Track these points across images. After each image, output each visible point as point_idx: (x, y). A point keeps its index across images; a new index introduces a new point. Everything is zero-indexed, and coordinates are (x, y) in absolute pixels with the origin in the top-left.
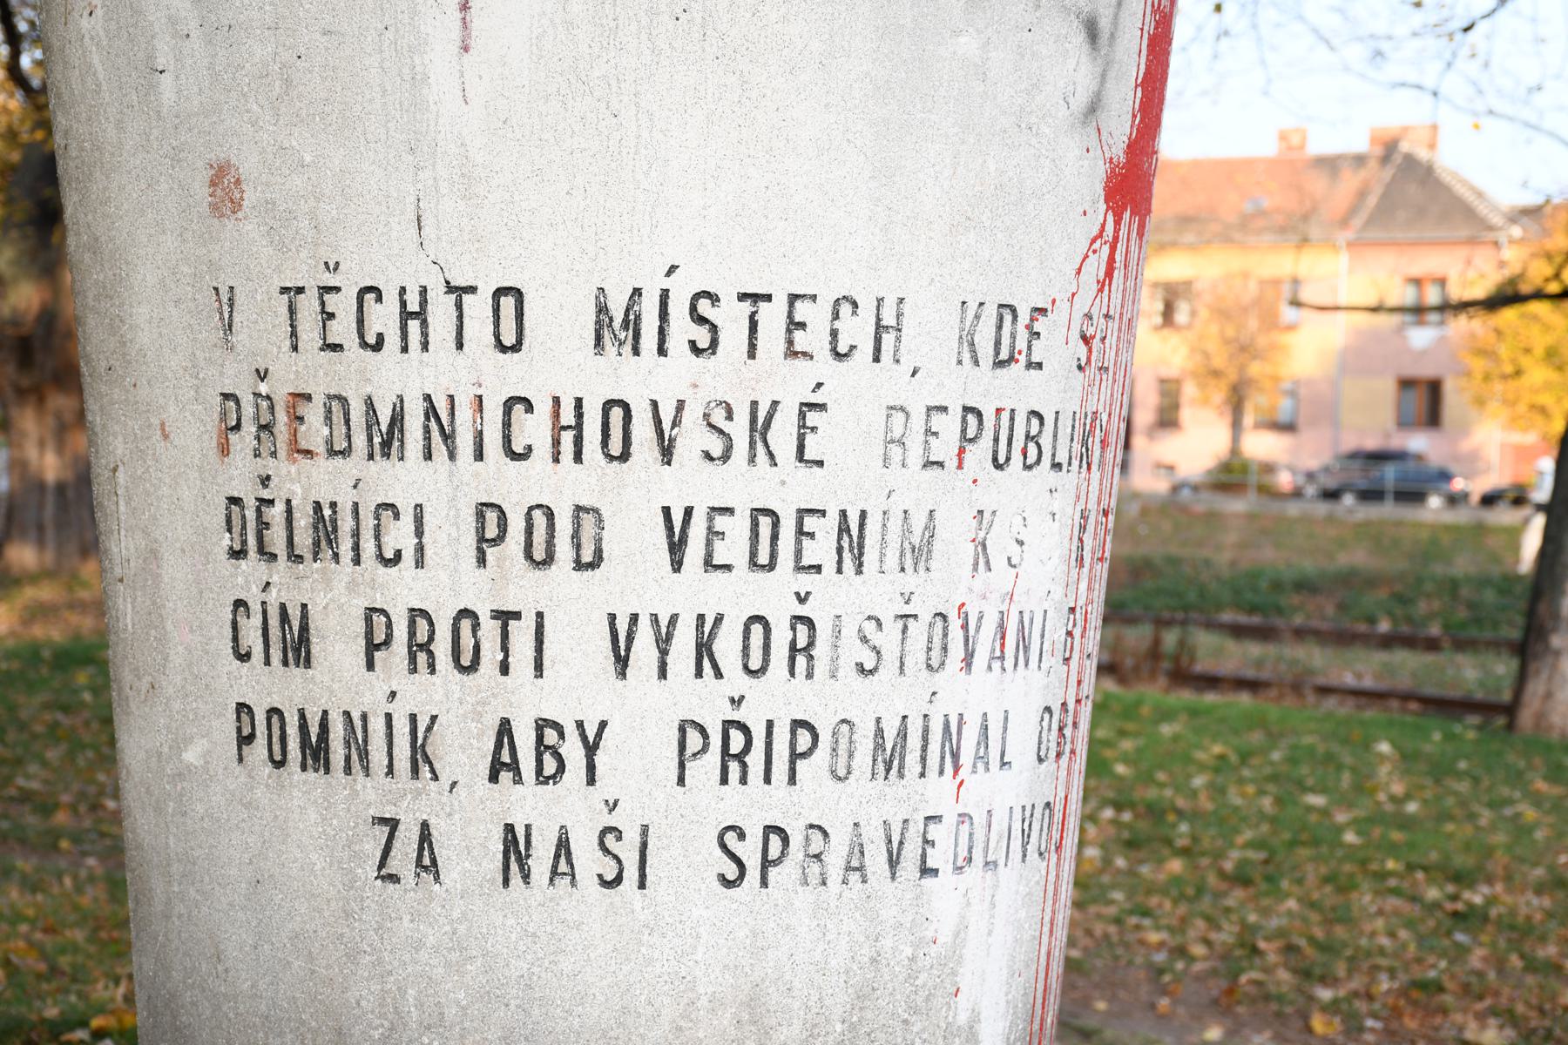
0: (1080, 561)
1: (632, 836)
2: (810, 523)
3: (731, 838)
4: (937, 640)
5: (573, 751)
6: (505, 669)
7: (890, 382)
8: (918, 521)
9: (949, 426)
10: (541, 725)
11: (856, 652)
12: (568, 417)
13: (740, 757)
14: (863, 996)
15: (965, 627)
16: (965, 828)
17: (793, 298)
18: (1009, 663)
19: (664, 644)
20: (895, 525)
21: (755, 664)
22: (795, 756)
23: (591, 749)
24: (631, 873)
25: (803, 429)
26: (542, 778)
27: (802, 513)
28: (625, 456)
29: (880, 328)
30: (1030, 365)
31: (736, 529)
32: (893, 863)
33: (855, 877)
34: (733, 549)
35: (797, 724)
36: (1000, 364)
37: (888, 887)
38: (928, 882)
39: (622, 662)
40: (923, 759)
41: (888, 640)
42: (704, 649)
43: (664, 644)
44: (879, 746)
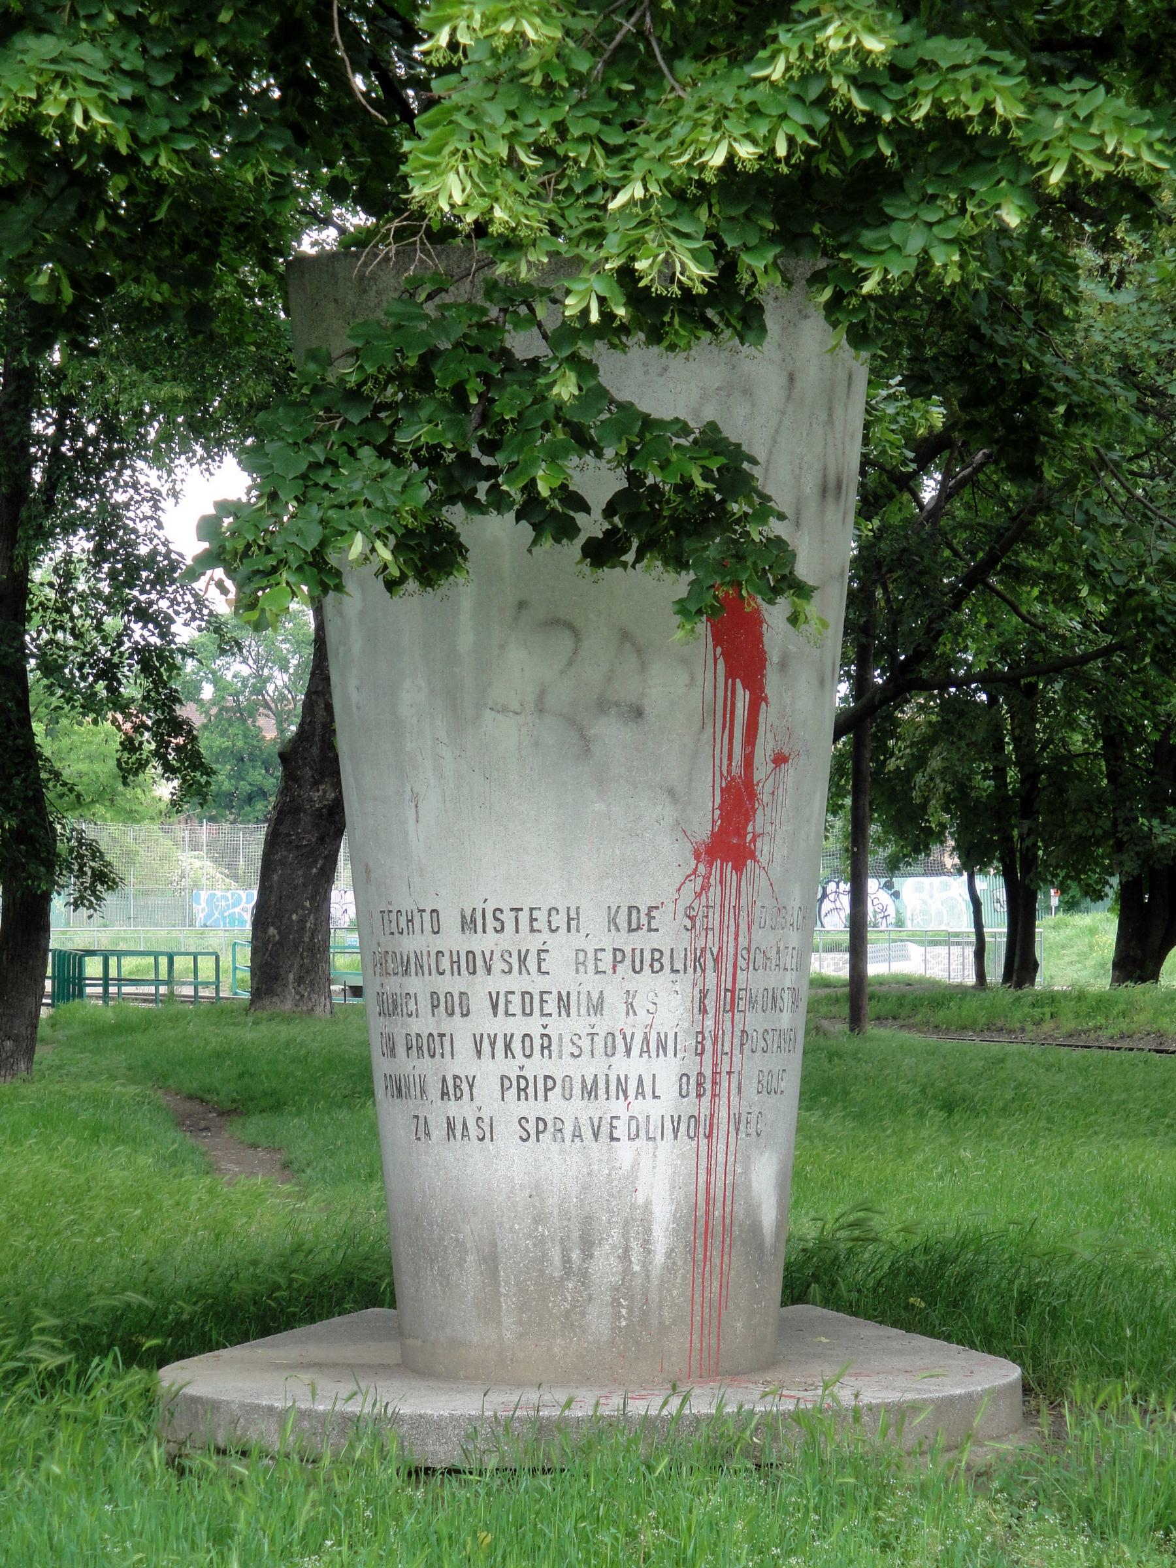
0: (704, 1011)
1: (487, 1120)
2: (545, 997)
3: (523, 1122)
4: (609, 1044)
5: (465, 1087)
6: (442, 1055)
7: (578, 940)
8: (595, 996)
9: (607, 958)
10: (455, 1077)
11: (568, 1048)
12: (455, 959)
13: (525, 1090)
14: (586, 1188)
15: (624, 1038)
16: (634, 1122)
17: (532, 909)
18: (653, 1054)
19: (493, 1045)
20: (583, 997)
21: (528, 1053)
22: (546, 1090)
23: (471, 1087)
24: (488, 1135)
25: (540, 961)
26: (457, 1099)
27: (542, 993)
28: (474, 972)
29: (569, 919)
30: (650, 930)
31: (516, 999)
32: (596, 1135)
33: (577, 1140)
34: (515, 1008)
35: (546, 1077)
36: (631, 930)
37: (594, 1144)
38: (614, 1143)
39: (479, 1052)
40: (607, 1092)
41: (585, 1043)
42: (508, 1047)
43: (493, 1045)
44: (584, 1086)
